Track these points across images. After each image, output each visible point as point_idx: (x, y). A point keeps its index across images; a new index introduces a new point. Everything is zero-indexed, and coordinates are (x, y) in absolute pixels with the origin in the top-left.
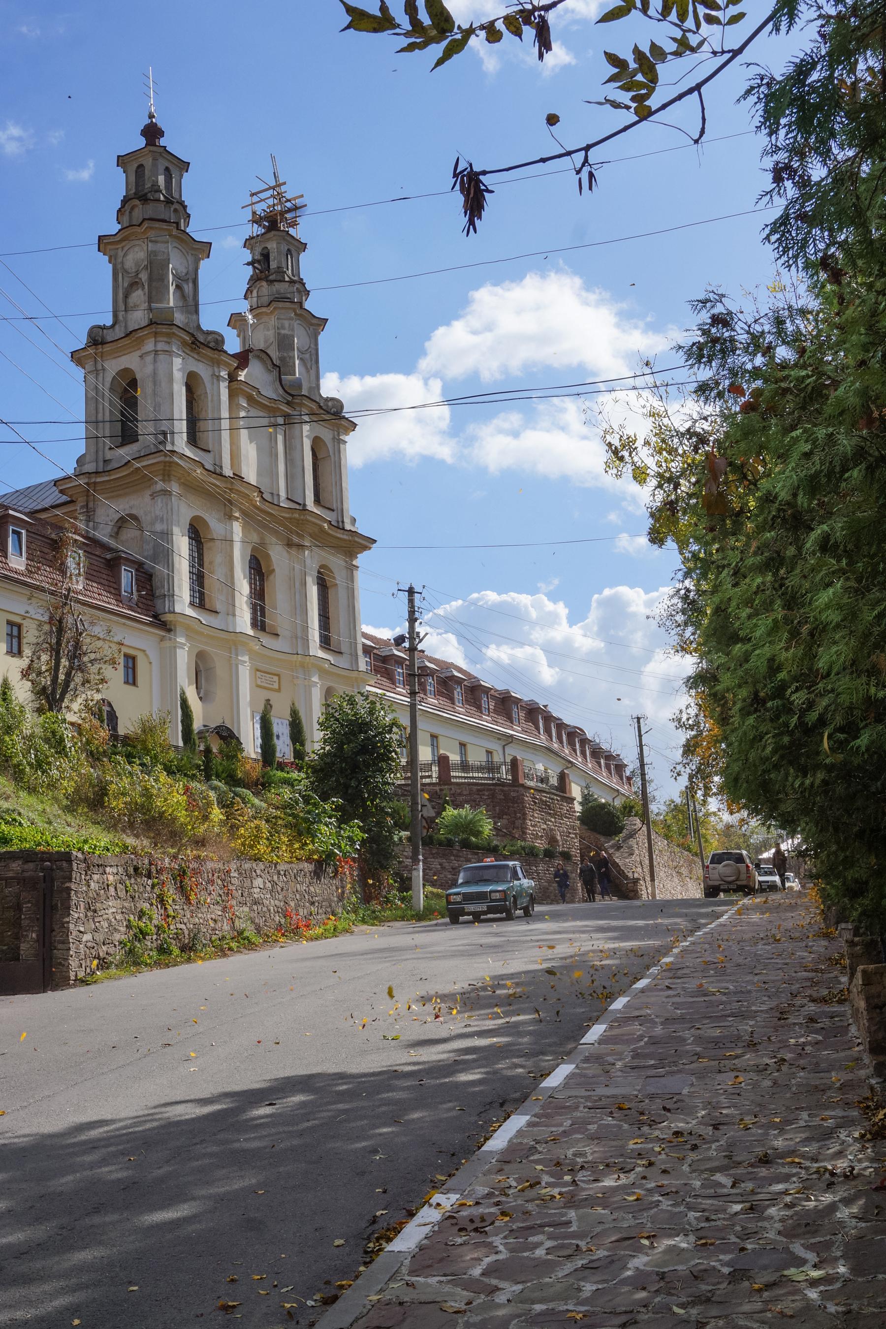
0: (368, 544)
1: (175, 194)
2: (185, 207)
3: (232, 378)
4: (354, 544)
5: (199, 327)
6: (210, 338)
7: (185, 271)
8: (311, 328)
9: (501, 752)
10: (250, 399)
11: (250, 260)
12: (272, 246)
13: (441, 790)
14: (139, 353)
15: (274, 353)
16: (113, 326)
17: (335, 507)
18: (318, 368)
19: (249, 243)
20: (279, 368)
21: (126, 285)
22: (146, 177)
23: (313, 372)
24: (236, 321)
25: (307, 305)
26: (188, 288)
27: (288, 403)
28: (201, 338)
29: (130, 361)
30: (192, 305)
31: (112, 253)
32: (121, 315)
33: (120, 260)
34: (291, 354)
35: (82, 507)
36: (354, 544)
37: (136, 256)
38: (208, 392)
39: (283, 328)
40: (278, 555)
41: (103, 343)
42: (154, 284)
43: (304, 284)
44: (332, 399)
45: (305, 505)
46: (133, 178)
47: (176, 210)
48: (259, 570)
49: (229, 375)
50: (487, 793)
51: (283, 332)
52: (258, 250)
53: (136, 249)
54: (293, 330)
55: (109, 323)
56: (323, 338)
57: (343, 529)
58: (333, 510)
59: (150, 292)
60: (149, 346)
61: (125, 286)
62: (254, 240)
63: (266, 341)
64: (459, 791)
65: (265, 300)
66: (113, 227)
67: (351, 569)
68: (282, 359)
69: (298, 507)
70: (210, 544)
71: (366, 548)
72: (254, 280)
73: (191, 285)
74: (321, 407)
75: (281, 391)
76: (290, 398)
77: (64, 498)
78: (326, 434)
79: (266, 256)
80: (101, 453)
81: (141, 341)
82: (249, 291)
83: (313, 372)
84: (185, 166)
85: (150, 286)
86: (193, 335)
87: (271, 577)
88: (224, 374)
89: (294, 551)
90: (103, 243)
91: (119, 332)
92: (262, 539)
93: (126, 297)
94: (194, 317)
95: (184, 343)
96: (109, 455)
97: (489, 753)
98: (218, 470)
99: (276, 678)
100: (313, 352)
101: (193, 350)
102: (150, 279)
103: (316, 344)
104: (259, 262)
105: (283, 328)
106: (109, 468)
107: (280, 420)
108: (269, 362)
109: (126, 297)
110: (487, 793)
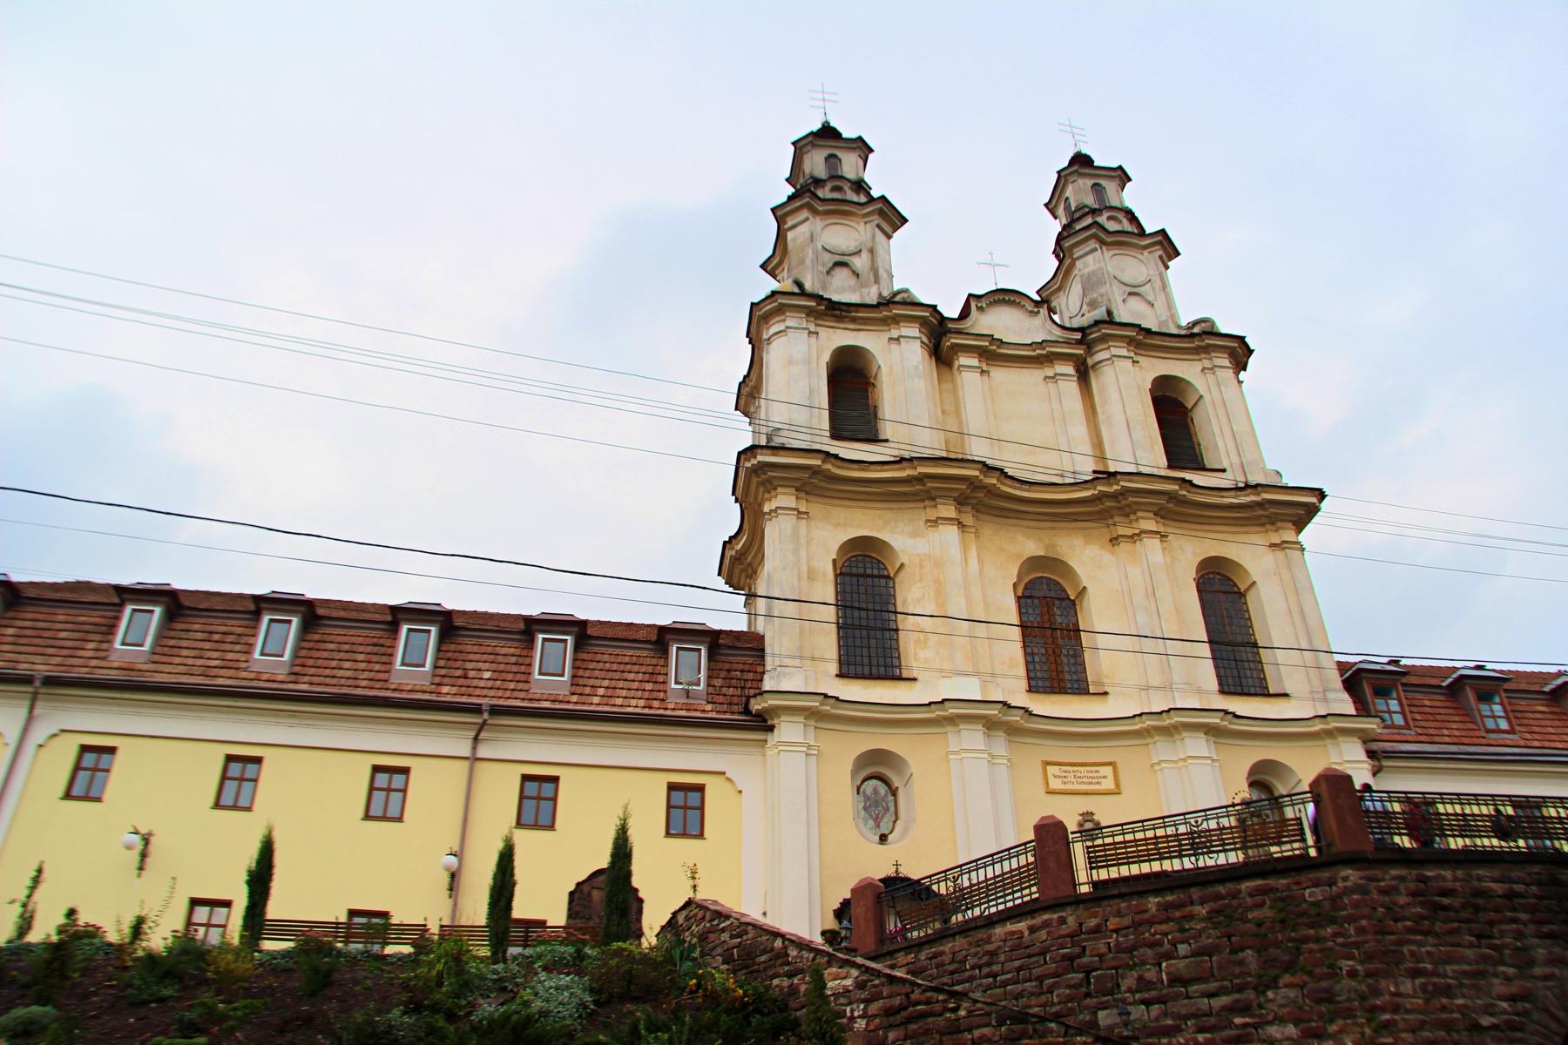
0: (1314, 500)
8: (1146, 253)
10: (983, 353)
13: (1032, 930)
17: (1225, 465)
27: (1079, 342)
34: (1103, 290)
38: (881, 363)
40: (1091, 562)
50: (1202, 910)
51: (1086, 271)
58: (1224, 471)
64: (1093, 922)
70: (902, 574)
71: (1312, 511)
73: (865, 255)
75: (1057, 332)
76: (1078, 336)
87: (1085, 603)
89: (1124, 546)
99: (1108, 770)
101: (840, 319)
110: (1202, 910)
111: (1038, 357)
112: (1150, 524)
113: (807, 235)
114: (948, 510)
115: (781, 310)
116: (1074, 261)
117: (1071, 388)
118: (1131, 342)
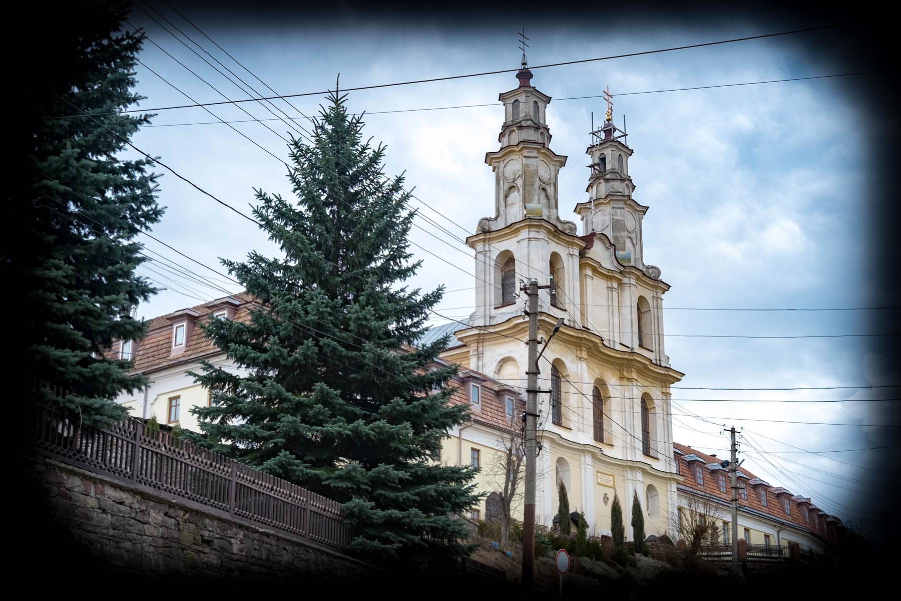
1: (541, 121)
2: (548, 130)
3: (582, 255)
4: (668, 377)
5: (558, 218)
6: (566, 226)
7: (548, 177)
9: (776, 536)
10: (594, 270)
11: (590, 162)
12: (608, 153)
14: (517, 239)
15: (610, 234)
16: (496, 218)
18: (641, 244)
19: (590, 150)
20: (612, 246)
21: (506, 188)
22: (521, 109)
23: (638, 247)
24: (580, 209)
25: (634, 196)
26: (550, 190)
27: (621, 272)
28: (560, 227)
29: (509, 244)
30: (553, 202)
31: (496, 165)
32: (502, 209)
33: (501, 170)
35: (474, 351)
36: (668, 377)
37: (514, 166)
39: (616, 214)
41: (489, 232)
42: (527, 188)
43: (631, 181)
44: (652, 267)
45: (632, 349)
46: (510, 110)
47: (542, 133)
48: (599, 398)
49: (580, 254)
51: (616, 218)
52: (597, 155)
53: (514, 162)
54: (623, 216)
55: (493, 216)
56: (647, 222)
57: (660, 366)
59: (524, 195)
60: (524, 234)
61: (505, 190)
62: (594, 150)
63: (603, 224)
65: (603, 194)
66: (496, 147)
67: (667, 394)
68: (615, 238)
69: (627, 350)
72: (595, 179)
73: (552, 187)
74: (644, 274)
75: (616, 263)
76: (622, 269)
77: (460, 343)
78: (648, 294)
79: (603, 160)
80: (487, 311)
81: (517, 231)
82: (590, 186)
83: (638, 247)
84: (548, 100)
85: (524, 189)
86: (556, 227)
87: (608, 402)
88: (576, 252)
89: (625, 382)
90: (489, 158)
91: (500, 224)
92: (602, 374)
93: (506, 197)
94: (555, 211)
95: (549, 232)
96: (494, 312)
97: (767, 536)
98: (572, 325)
100: (638, 232)
101: (555, 236)
102: (524, 185)
103: (640, 226)
104: (598, 164)
105: (616, 214)
106: (493, 323)
107: (615, 285)
108: (607, 242)
109: (506, 197)
111: (608, 276)
112: (634, 375)
113: (535, 168)
114: (584, 355)
115: (539, 227)
116: (608, 203)
117: (615, 294)
118: (638, 278)
